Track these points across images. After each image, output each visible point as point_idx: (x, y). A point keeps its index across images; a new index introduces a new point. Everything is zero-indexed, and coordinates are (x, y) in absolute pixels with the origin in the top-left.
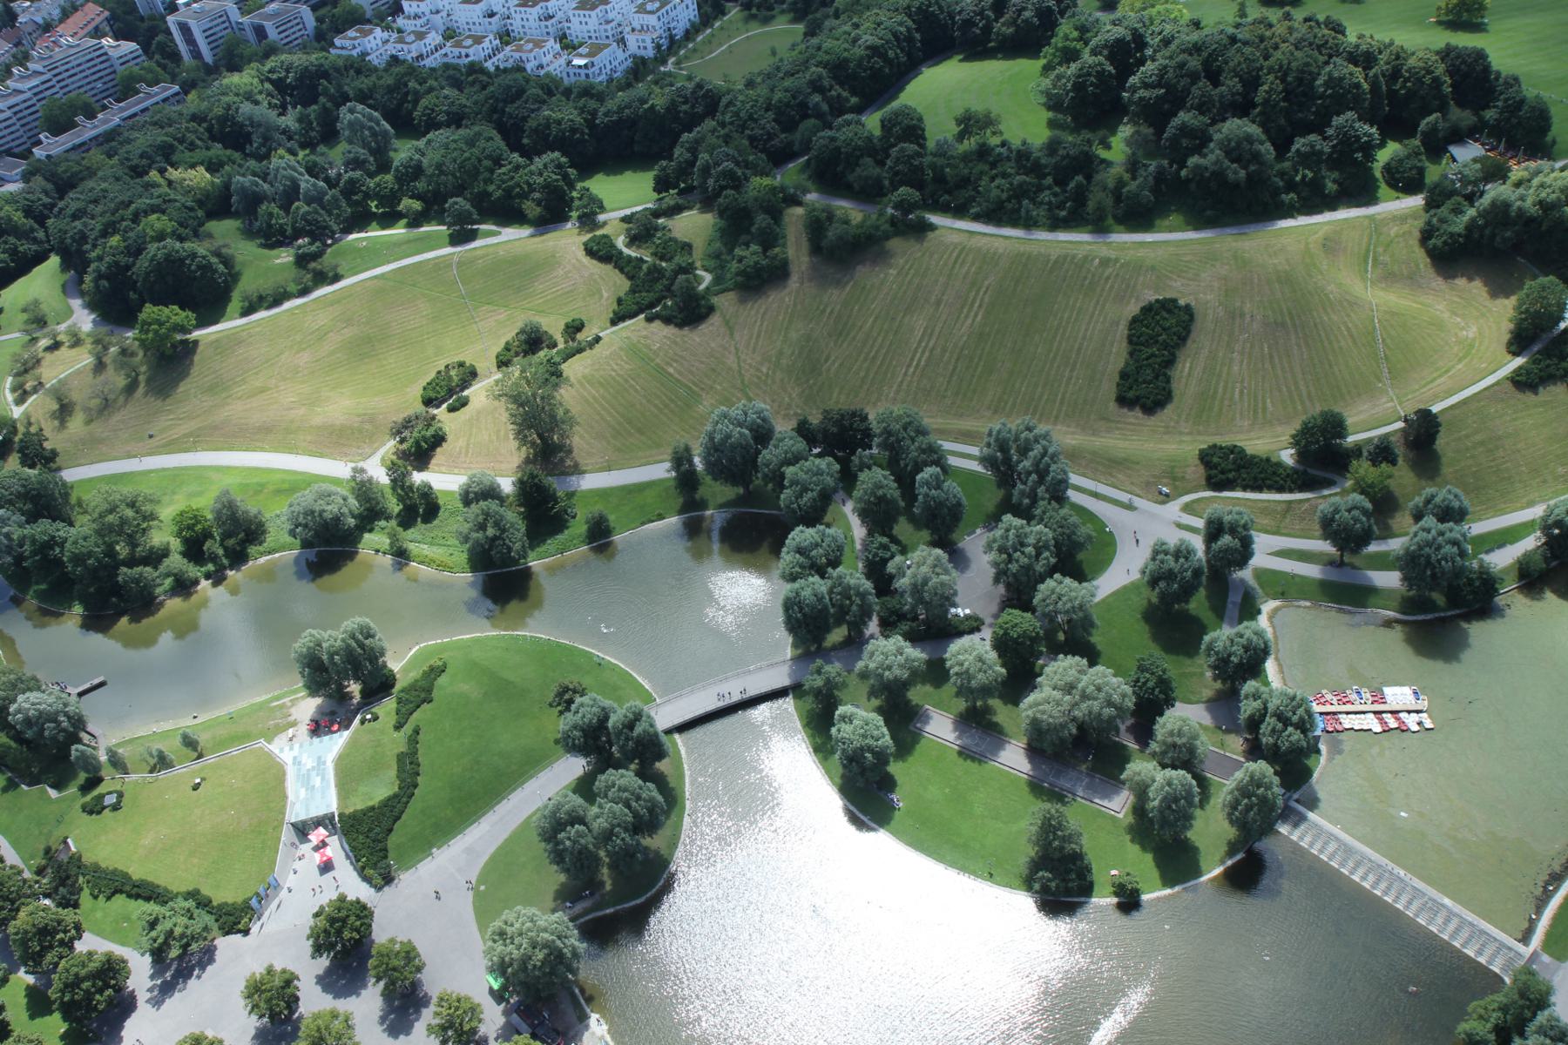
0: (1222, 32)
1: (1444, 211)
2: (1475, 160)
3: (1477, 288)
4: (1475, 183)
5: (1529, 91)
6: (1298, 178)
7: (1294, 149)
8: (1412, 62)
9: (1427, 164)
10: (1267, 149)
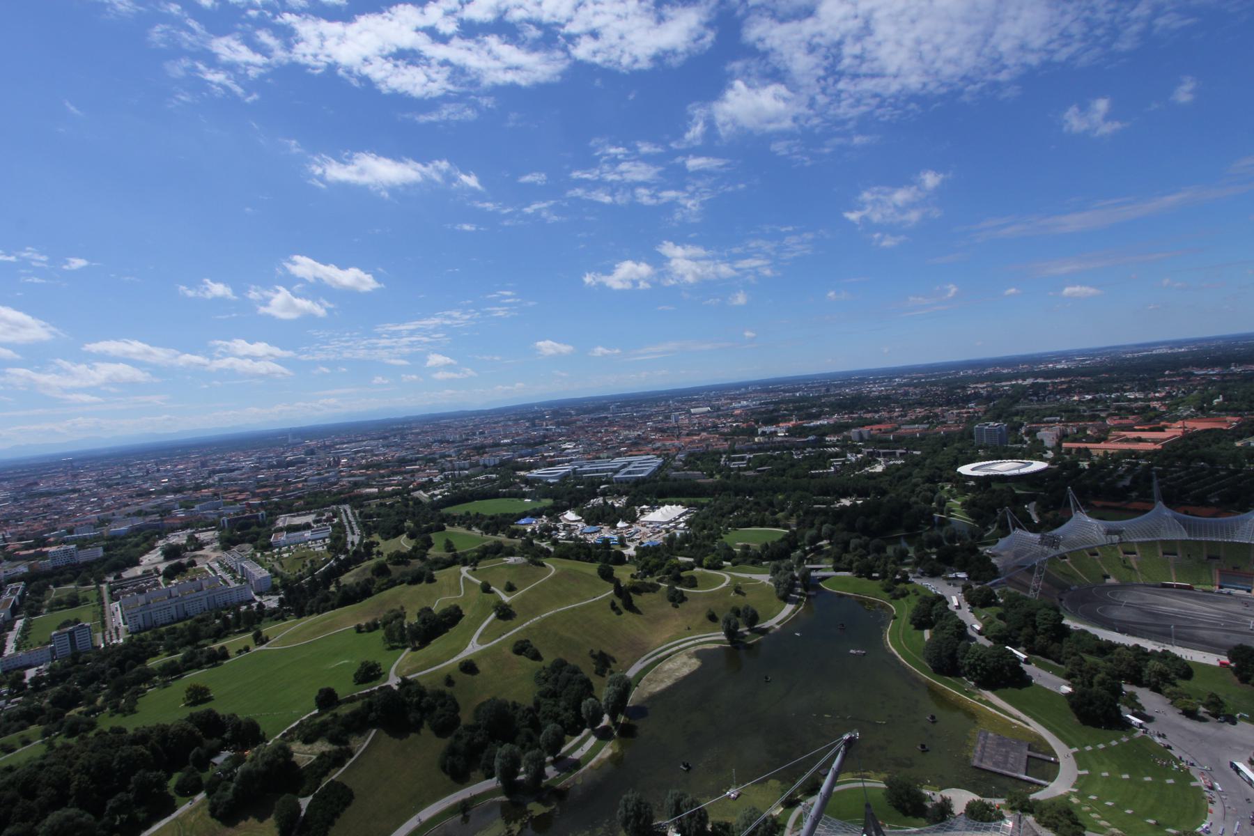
0: (31, 766)
1: (218, 792)
2: (226, 760)
3: (252, 821)
4: (231, 770)
5: (241, 717)
6: (117, 823)
7: (108, 808)
8: (172, 729)
9: (201, 774)
10: (87, 817)
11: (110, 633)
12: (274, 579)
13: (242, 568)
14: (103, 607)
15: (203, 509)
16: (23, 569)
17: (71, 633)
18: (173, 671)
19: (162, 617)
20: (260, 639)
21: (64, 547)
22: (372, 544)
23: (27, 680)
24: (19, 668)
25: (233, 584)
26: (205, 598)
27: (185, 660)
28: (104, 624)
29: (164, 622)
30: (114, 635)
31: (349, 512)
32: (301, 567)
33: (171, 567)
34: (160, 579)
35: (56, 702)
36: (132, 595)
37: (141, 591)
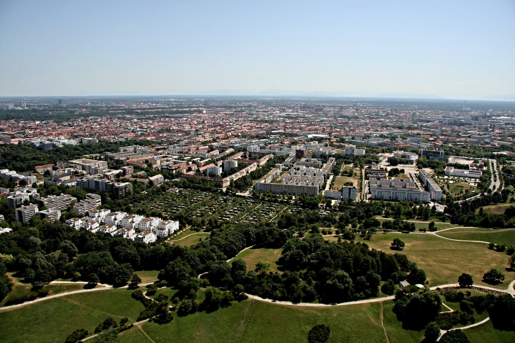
11: (364, 195)
12: (443, 195)
13: (428, 182)
14: (362, 181)
15: (411, 141)
16: (335, 152)
17: (350, 189)
18: (387, 226)
19: (386, 196)
20: (432, 228)
21: (351, 145)
22: (508, 192)
23: (332, 204)
24: (330, 198)
25: (422, 190)
26: (407, 192)
27: (394, 223)
28: (361, 189)
29: (386, 199)
30: (365, 198)
31: (495, 165)
32: (459, 193)
33: (392, 170)
34: (387, 174)
35: (341, 219)
36: (375, 179)
37: (379, 179)
